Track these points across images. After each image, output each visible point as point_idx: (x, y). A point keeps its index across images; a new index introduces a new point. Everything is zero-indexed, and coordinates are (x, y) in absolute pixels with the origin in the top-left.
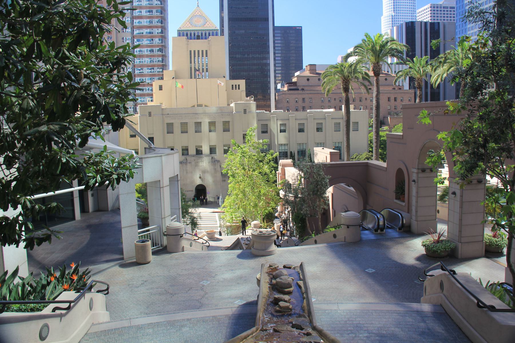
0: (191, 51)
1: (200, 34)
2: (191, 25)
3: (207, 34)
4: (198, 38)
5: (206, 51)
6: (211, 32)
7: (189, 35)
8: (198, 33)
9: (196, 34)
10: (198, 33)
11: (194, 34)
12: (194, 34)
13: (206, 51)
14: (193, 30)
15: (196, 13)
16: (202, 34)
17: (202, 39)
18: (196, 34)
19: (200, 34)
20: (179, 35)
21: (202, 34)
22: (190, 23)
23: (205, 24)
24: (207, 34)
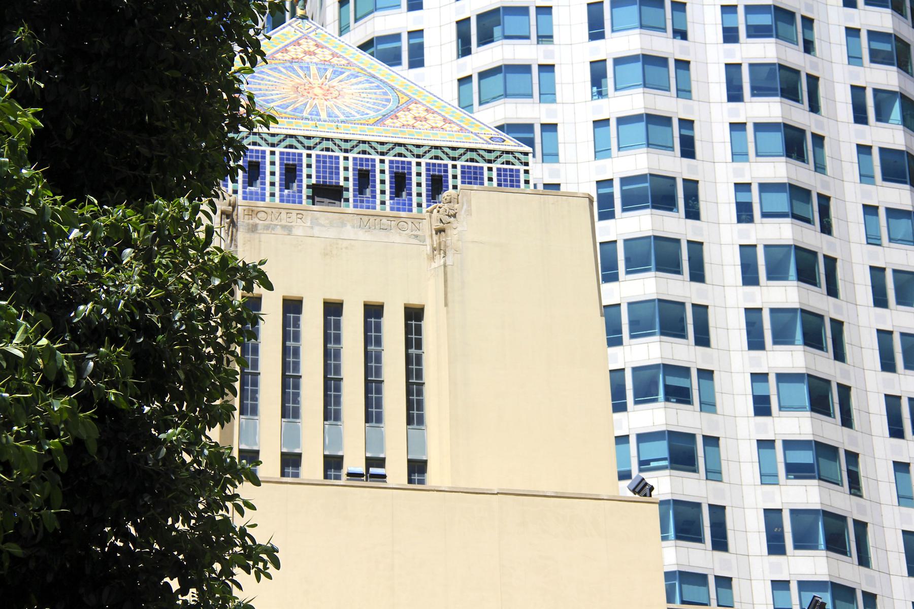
1: (346, 178)
3: (419, 182)
4: (328, 192)
5: (414, 315)
6: (454, 170)
8: (328, 165)
9: (309, 176)
10: (328, 165)
12: (291, 173)
13: (414, 315)
15: (293, 52)
16: (364, 179)
18: (309, 176)
19: (346, 178)
21: (364, 179)
23: (393, 114)
24: (419, 182)
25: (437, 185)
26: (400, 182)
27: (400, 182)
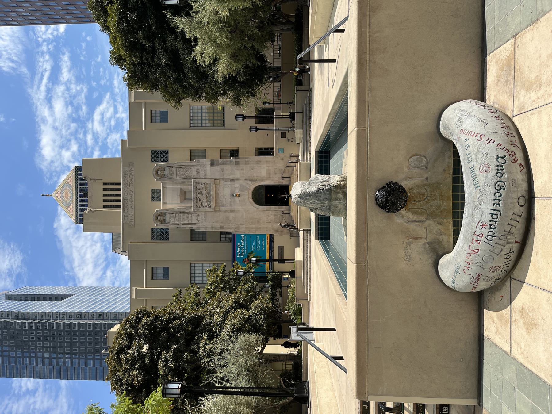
0: (105, 207)
1: (82, 193)
2: (70, 205)
4: (85, 195)
5: (104, 184)
6: (79, 177)
7: (83, 208)
8: (80, 195)
9: (82, 198)
10: (80, 195)
11: (82, 200)
12: (82, 200)
13: (104, 184)
14: (77, 203)
17: (87, 190)
18: (82, 198)
19: (82, 193)
20: (81, 222)
22: (69, 207)
25: (82, 180)
26: (82, 185)
27: (82, 185)
